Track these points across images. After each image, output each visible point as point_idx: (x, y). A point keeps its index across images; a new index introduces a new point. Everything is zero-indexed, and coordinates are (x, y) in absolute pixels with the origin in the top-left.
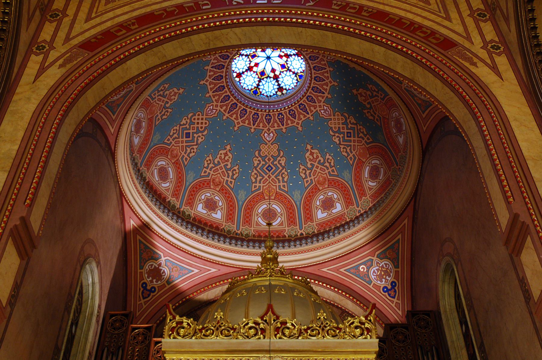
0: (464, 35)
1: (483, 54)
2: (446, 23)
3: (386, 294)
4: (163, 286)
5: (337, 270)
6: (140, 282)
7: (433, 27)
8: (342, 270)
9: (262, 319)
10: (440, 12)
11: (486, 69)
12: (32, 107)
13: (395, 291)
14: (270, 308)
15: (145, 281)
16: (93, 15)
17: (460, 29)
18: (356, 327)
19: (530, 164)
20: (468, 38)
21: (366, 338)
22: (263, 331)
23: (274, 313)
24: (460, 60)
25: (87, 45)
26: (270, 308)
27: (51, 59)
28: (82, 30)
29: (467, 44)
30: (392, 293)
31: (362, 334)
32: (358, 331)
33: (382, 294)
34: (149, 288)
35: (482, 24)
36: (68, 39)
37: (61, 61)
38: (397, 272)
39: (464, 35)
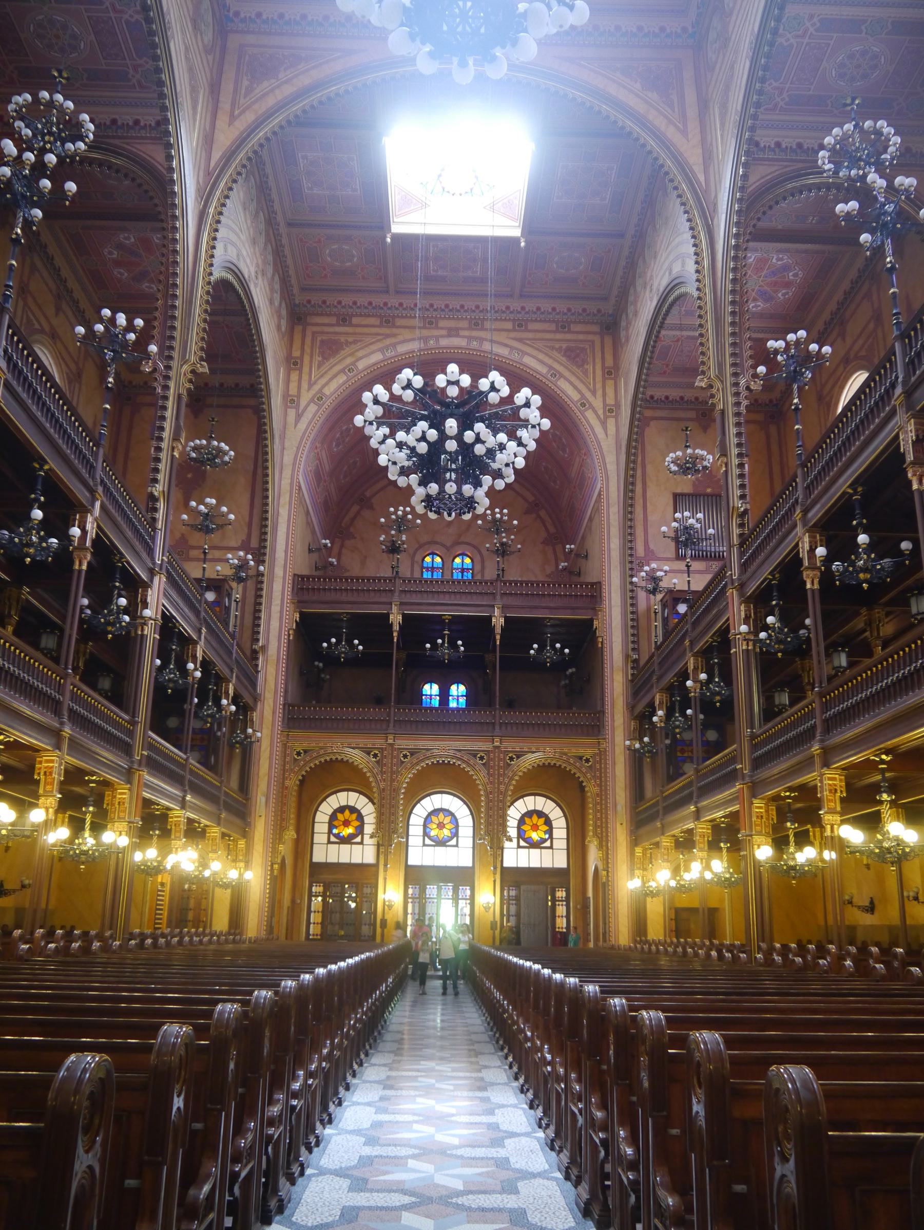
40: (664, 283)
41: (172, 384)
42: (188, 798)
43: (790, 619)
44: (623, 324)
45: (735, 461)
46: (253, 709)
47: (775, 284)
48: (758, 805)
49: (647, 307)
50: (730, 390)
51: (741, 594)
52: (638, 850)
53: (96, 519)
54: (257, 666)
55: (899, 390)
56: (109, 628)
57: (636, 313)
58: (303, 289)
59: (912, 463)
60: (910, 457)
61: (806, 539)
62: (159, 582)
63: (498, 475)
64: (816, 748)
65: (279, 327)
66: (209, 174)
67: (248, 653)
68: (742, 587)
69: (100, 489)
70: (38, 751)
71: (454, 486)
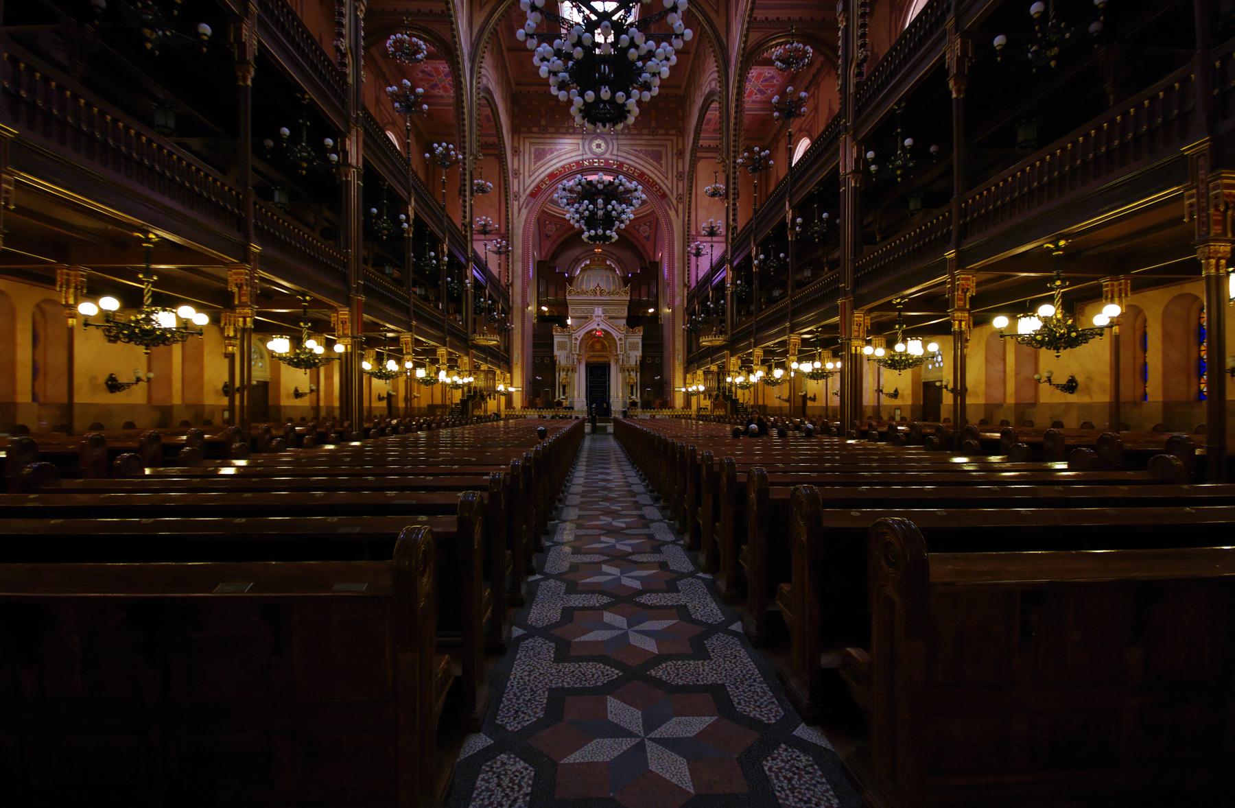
0: (671, 189)
1: (675, 202)
2: (666, 182)
11: (674, 212)
12: (521, 231)
14: (598, 285)
17: (670, 186)
19: (676, 261)
20: (672, 192)
25: (533, 195)
26: (598, 285)
27: (521, 203)
29: (671, 197)
35: (679, 183)
36: (525, 190)
37: (524, 206)
39: (671, 189)
40: (707, 91)
41: (467, 167)
42: (489, 358)
43: (748, 281)
44: (688, 103)
45: (731, 202)
46: (509, 314)
47: (768, 86)
48: (733, 360)
49: (700, 102)
50: (732, 165)
51: (731, 267)
52: (688, 376)
53: (413, 208)
54: (509, 293)
55: (787, 195)
56: (426, 268)
57: (694, 102)
58: (518, 84)
59: (790, 229)
60: (789, 226)
61: (755, 249)
62: (471, 264)
63: (622, 222)
64: (752, 340)
65: (507, 111)
66: (472, 44)
67: (504, 286)
68: (731, 262)
69: (447, 231)
70: (437, 347)
71: (602, 231)
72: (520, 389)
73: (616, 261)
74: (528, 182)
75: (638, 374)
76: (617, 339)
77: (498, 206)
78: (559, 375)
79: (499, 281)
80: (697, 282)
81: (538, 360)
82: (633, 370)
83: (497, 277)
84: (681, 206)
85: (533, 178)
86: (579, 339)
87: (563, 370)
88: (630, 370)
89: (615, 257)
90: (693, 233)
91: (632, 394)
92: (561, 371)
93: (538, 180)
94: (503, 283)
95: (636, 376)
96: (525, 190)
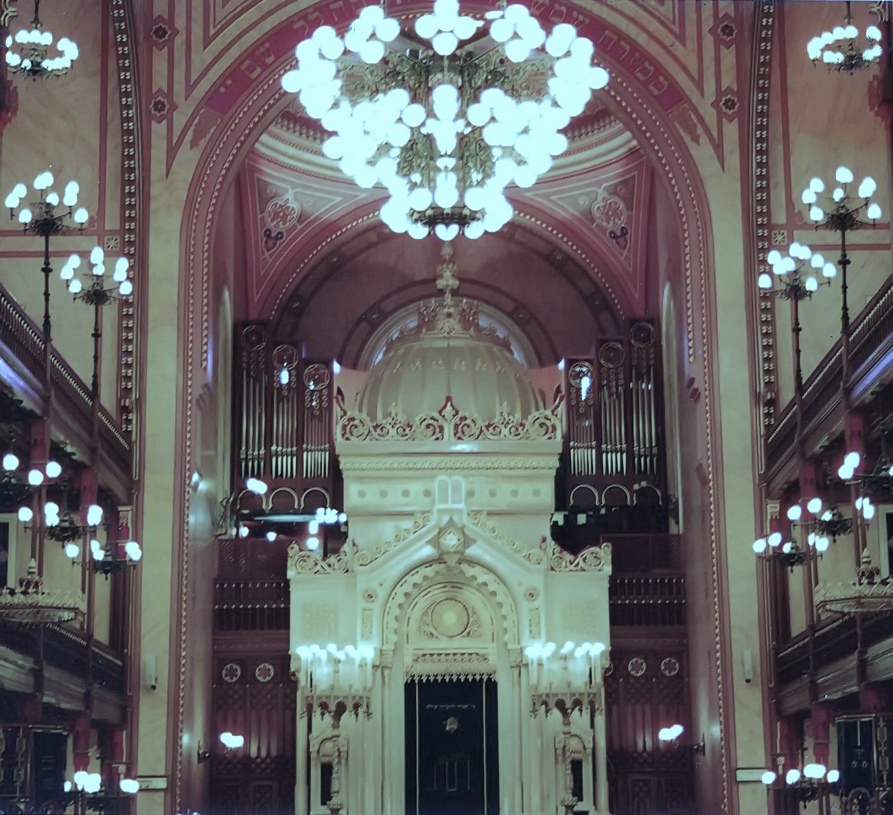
0: (696, 76)
1: (710, 115)
3: (614, 241)
4: (294, 227)
5: (547, 196)
6: (261, 230)
7: (659, 58)
8: (554, 198)
9: (440, 414)
10: (674, 23)
13: (626, 240)
14: (449, 399)
15: (268, 227)
16: (212, 31)
18: (541, 425)
20: (699, 84)
21: (550, 438)
22: (441, 429)
23: (452, 405)
24: (681, 131)
26: (449, 399)
28: (205, 66)
29: (694, 96)
30: (623, 243)
31: (546, 433)
32: (543, 431)
33: (607, 239)
34: (274, 234)
35: (724, 51)
36: (190, 87)
38: (629, 218)
39: (696, 76)
72: (161, 783)
73: (511, 315)
74: (201, 58)
75: (600, 720)
76: (520, 592)
77: (95, 141)
78: (310, 730)
79: (94, 393)
80: (800, 388)
81: (232, 673)
82: (577, 703)
83: (88, 381)
84: (731, 131)
85: (217, 45)
86: (381, 594)
87: (324, 706)
88: (568, 704)
89: (510, 306)
90: (780, 217)
91: (578, 792)
92: (317, 711)
93: (235, 52)
94: (107, 398)
95: (592, 726)
96: (190, 87)
